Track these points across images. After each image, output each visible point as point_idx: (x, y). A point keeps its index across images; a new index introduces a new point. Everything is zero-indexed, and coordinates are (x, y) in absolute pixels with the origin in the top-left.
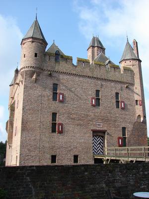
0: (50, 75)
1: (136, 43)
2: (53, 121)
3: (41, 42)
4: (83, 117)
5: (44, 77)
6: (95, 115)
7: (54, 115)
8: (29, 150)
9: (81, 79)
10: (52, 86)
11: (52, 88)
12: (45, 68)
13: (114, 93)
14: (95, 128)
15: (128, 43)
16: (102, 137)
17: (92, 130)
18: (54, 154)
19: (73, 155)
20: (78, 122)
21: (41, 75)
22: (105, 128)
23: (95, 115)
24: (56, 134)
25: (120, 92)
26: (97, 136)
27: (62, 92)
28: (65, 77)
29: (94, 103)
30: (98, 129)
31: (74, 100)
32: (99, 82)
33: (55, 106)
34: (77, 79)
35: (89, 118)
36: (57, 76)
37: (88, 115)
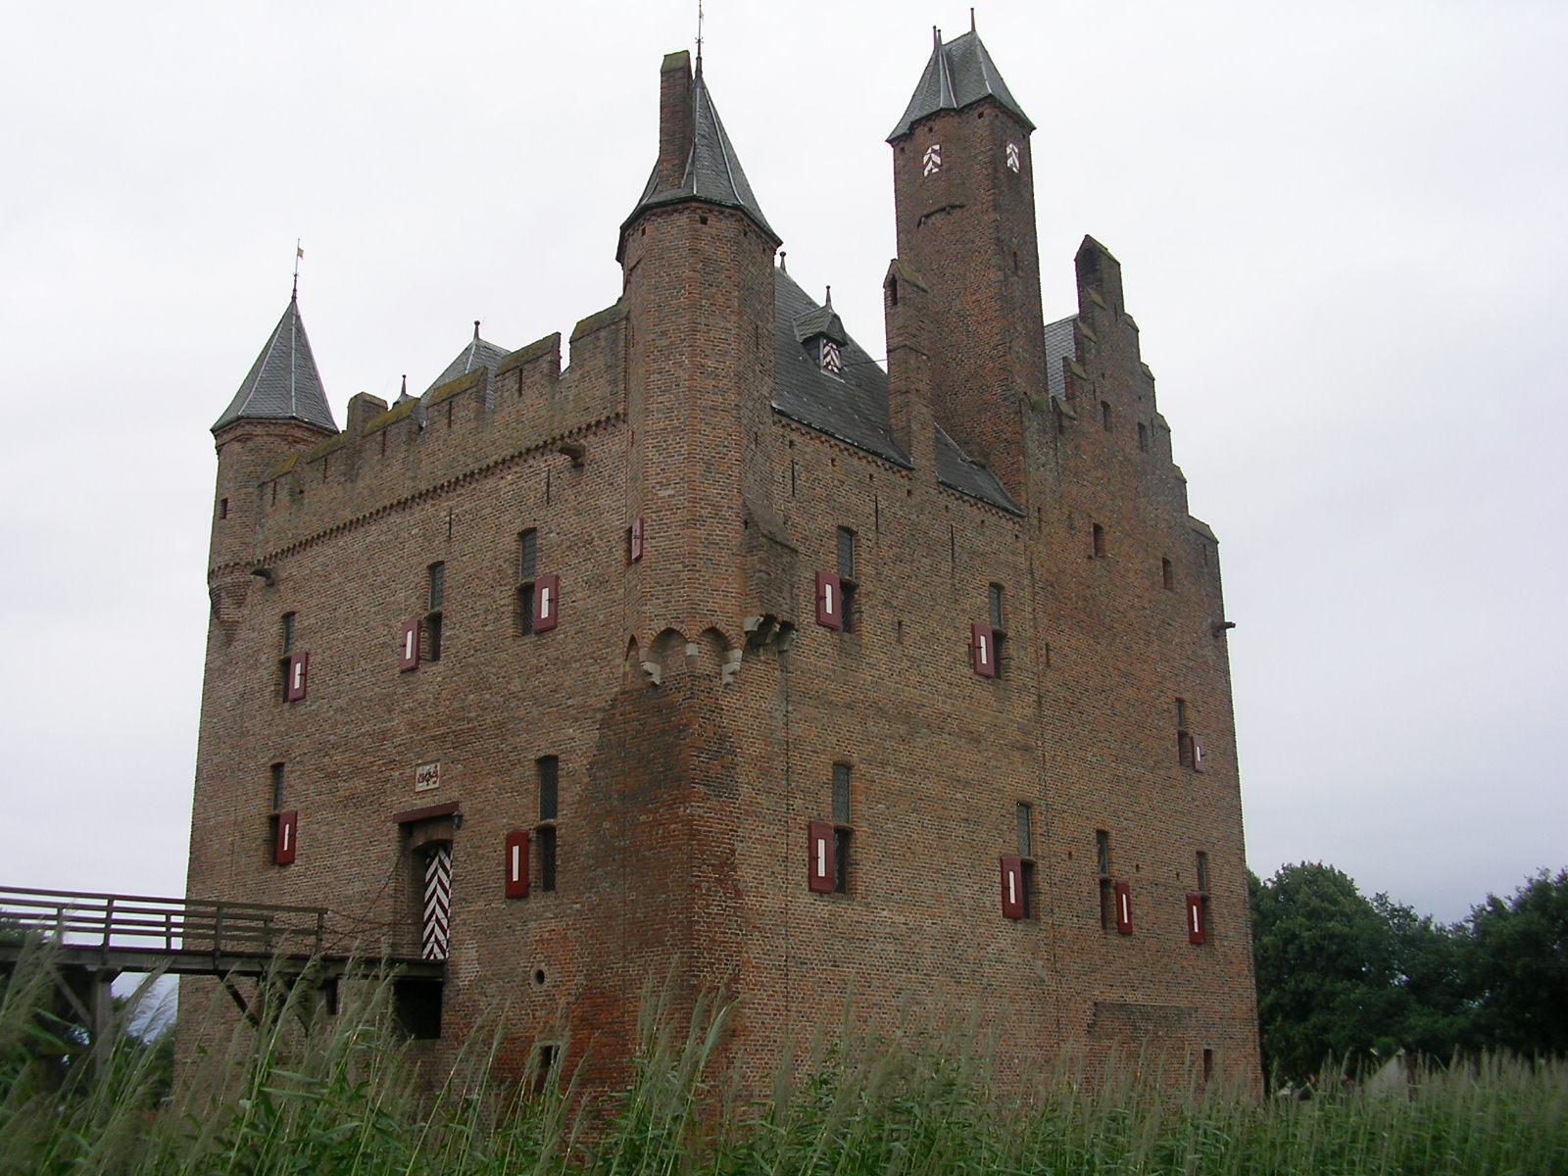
3: (239, 432)
30: (420, 803)
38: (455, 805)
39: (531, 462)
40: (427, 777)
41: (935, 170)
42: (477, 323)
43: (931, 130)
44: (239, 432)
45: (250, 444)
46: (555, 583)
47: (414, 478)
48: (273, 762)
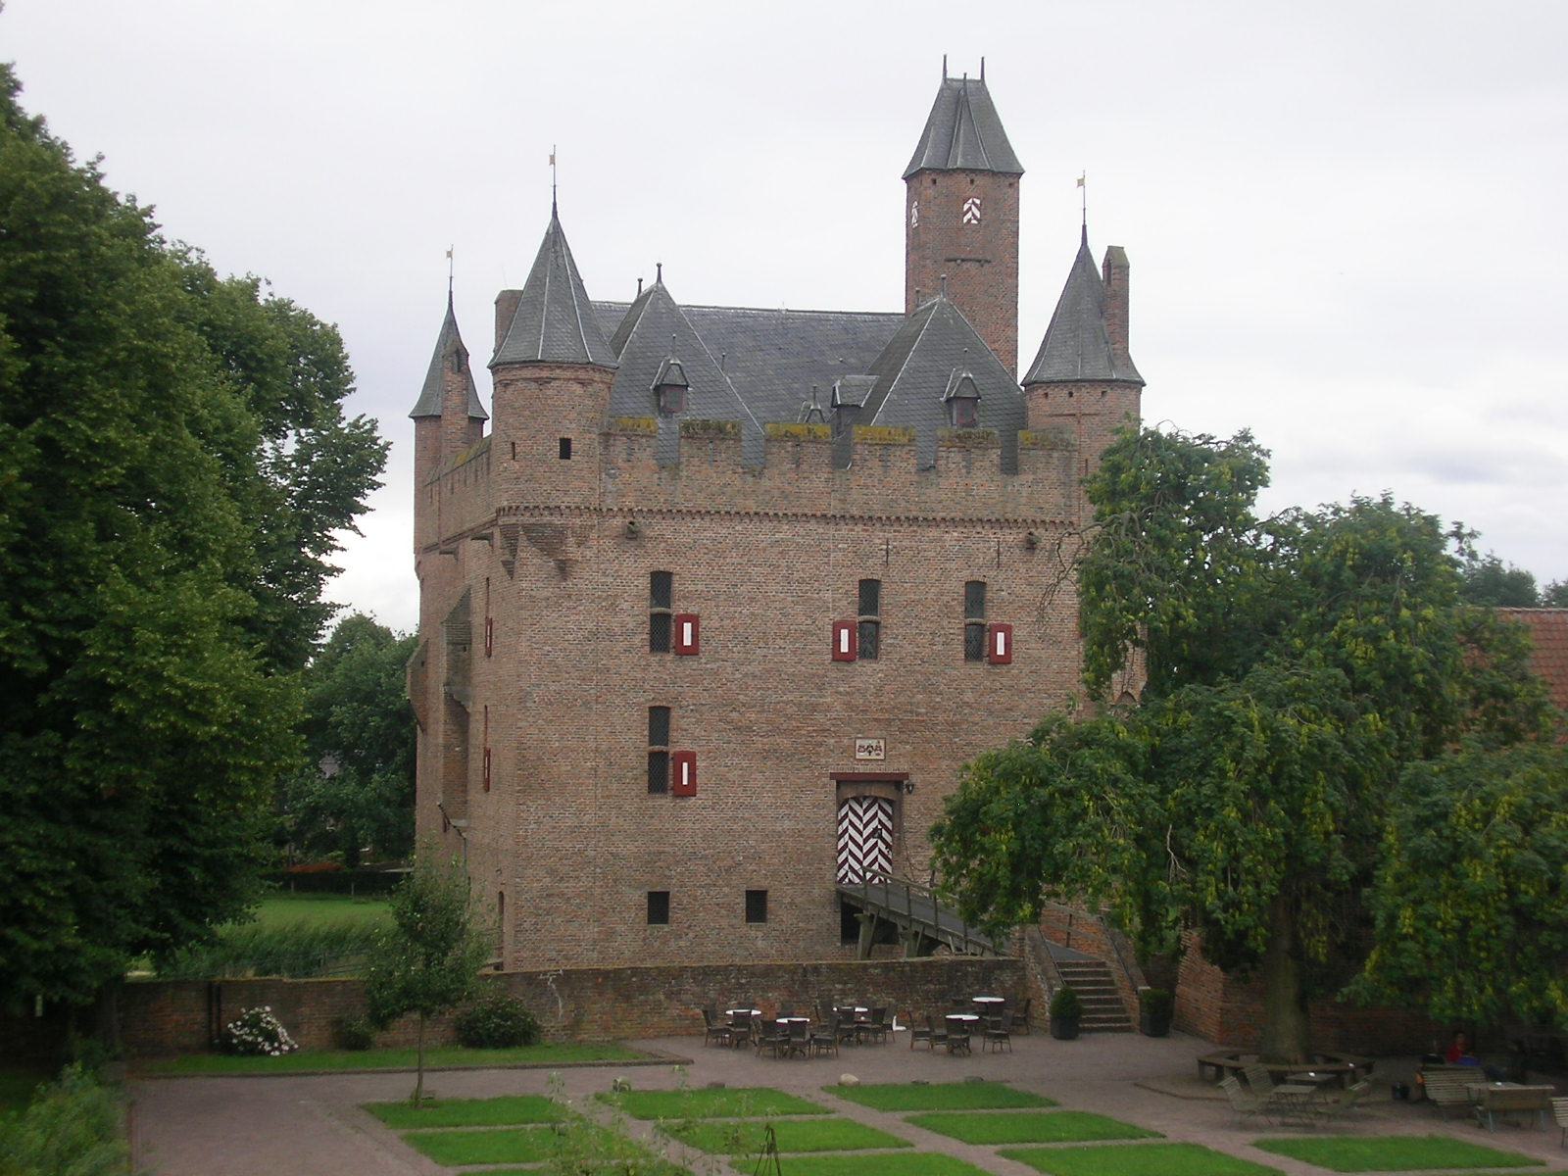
0: (632, 534)
1: (1117, 261)
2: (651, 742)
3: (582, 375)
4: (789, 718)
5: (608, 543)
6: (850, 707)
7: (659, 719)
8: (552, 872)
9: (785, 531)
10: (645, 583)
11: (647, 593)
12: (609, 502)
13: (956, 587)
14: (846, 767)
15: (1084, 256)
16: (890, 802)
17: (833, 776)
18: (658, 889)
19: (744, 888)
20: (760, 743)
21: (594, 535)
22: (903, 766)
23: (850, 707)
24: (665, 802)
25: (989, 576)
26: (865, 798)
27: (693, 610)
28: (711, 531)
29: (844, 648)
30: (861, 769)
31: (746, 641)
32: (879, 537)
33: (662, 675)
34: (763, 534)
35: (818, 716)
36: (668, 535)
37: (814, 708)
38: (906, 776)
39: (979, 529)
40: (869, 749)
41: (974, 222)
42: (659, 266)
43: (972, 181)
44: (582, 375)
45: (590, 389)
46: (1007, 630)
47: (843, 501)
48: (653, 704)
